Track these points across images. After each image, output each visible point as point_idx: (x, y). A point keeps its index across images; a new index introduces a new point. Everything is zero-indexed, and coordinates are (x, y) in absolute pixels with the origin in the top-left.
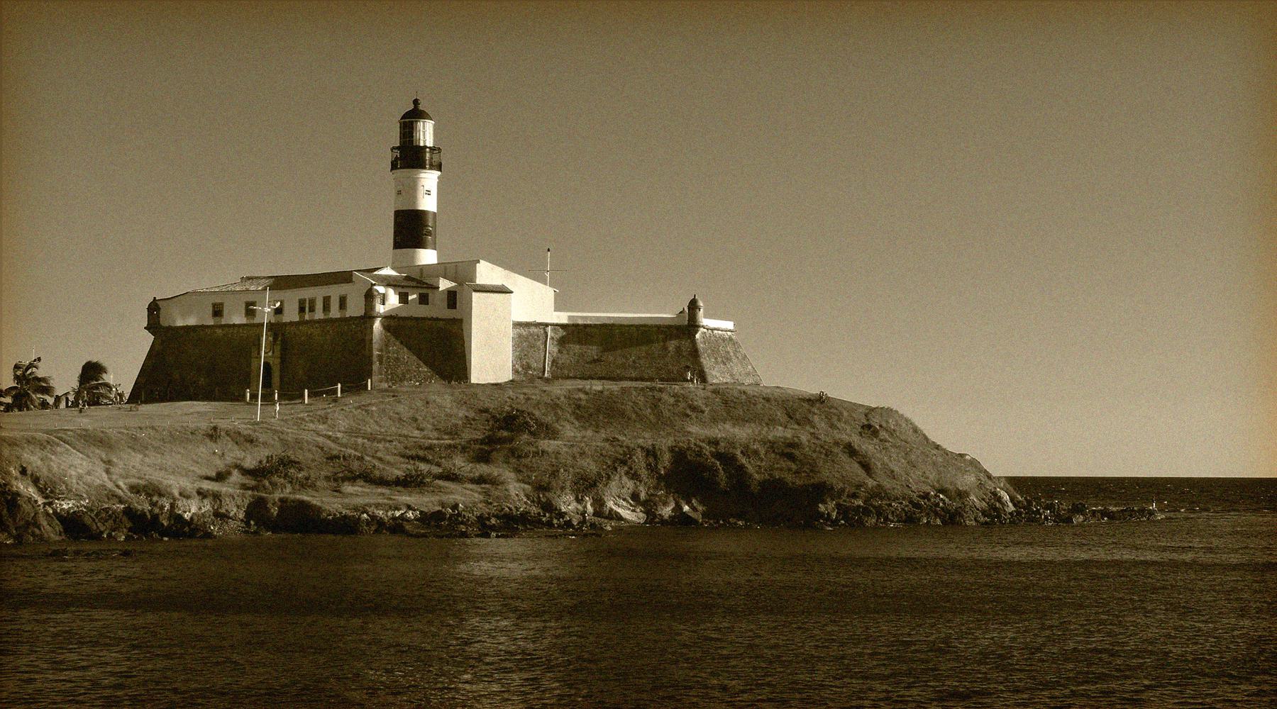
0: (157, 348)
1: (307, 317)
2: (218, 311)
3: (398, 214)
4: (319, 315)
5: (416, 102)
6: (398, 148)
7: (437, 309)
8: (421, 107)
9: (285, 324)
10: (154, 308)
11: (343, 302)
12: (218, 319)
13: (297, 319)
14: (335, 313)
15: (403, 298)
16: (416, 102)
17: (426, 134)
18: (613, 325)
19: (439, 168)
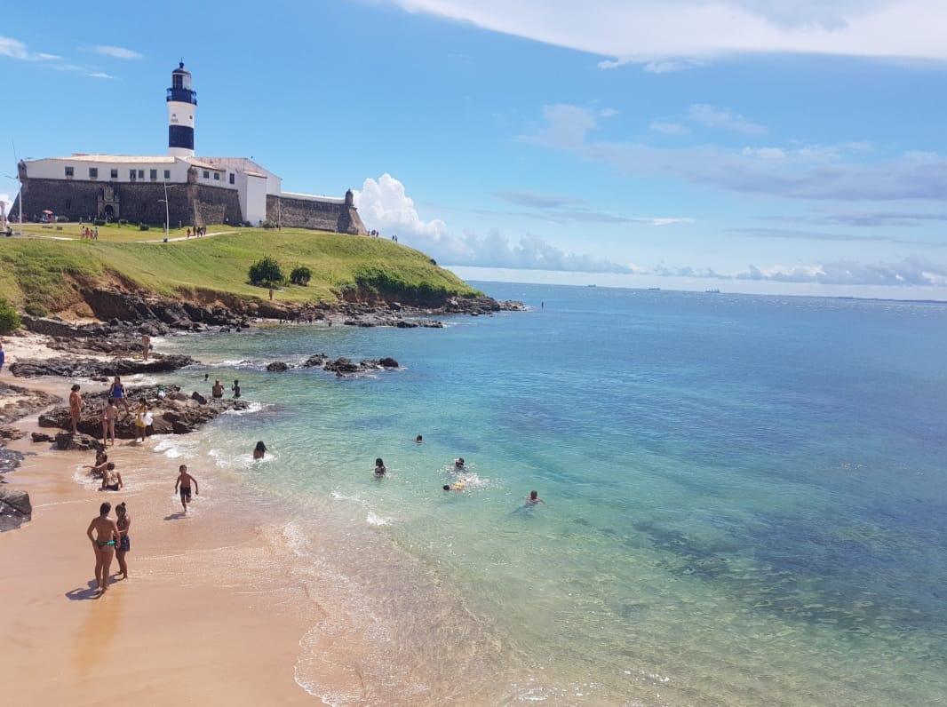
0: (27, 190)
1: (137, 180)
2: (69, 171)
3: (172, 128)
4: (147, 179)
5: (182, 65)
6: (170, 89)
7: (224, 183)
8: (185, 69)
9: (120, 183)
10: (22, 167)
11: (167, 174)
13: (129, 181)
14: (161, 178)
15: (206, 175)
16: (182, 65)
17: (188, 84)
18: (309, 201)
19: (195, 103)
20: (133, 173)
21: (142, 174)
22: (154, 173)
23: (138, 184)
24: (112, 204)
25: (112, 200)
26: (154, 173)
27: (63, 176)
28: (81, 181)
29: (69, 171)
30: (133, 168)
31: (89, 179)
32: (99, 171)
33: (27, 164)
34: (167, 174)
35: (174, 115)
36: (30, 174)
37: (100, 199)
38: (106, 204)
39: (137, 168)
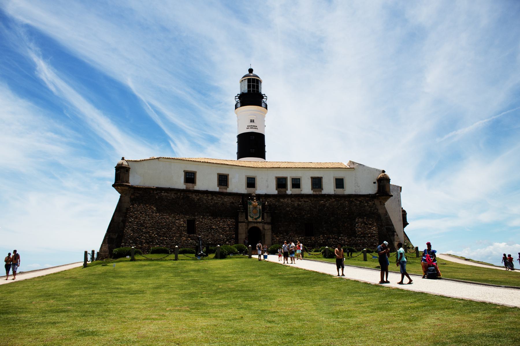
2: (190, 177)
4: (306, 188)
5: (251, 71)
11: (339, 183)
12: (190, 186)
13: (276, 192)
14: (329, 188)
20: (281, 183)
21: (296, 183)
22: (317, 182)
23: (291, 196)
24: (260, 226)
25: (260, 220)
26: (317, 182)
27: (180, 183)
28: (206, 192)
29: (190, 177)
30: (281, 174)
31: (217, 189)
32: (230, 177)
33: (131, 165)
34: (339, 183)
35: (253, 121)
36: (135, 180)
37: (241, 218)
38: (251, 226)
39: (289, 175)
